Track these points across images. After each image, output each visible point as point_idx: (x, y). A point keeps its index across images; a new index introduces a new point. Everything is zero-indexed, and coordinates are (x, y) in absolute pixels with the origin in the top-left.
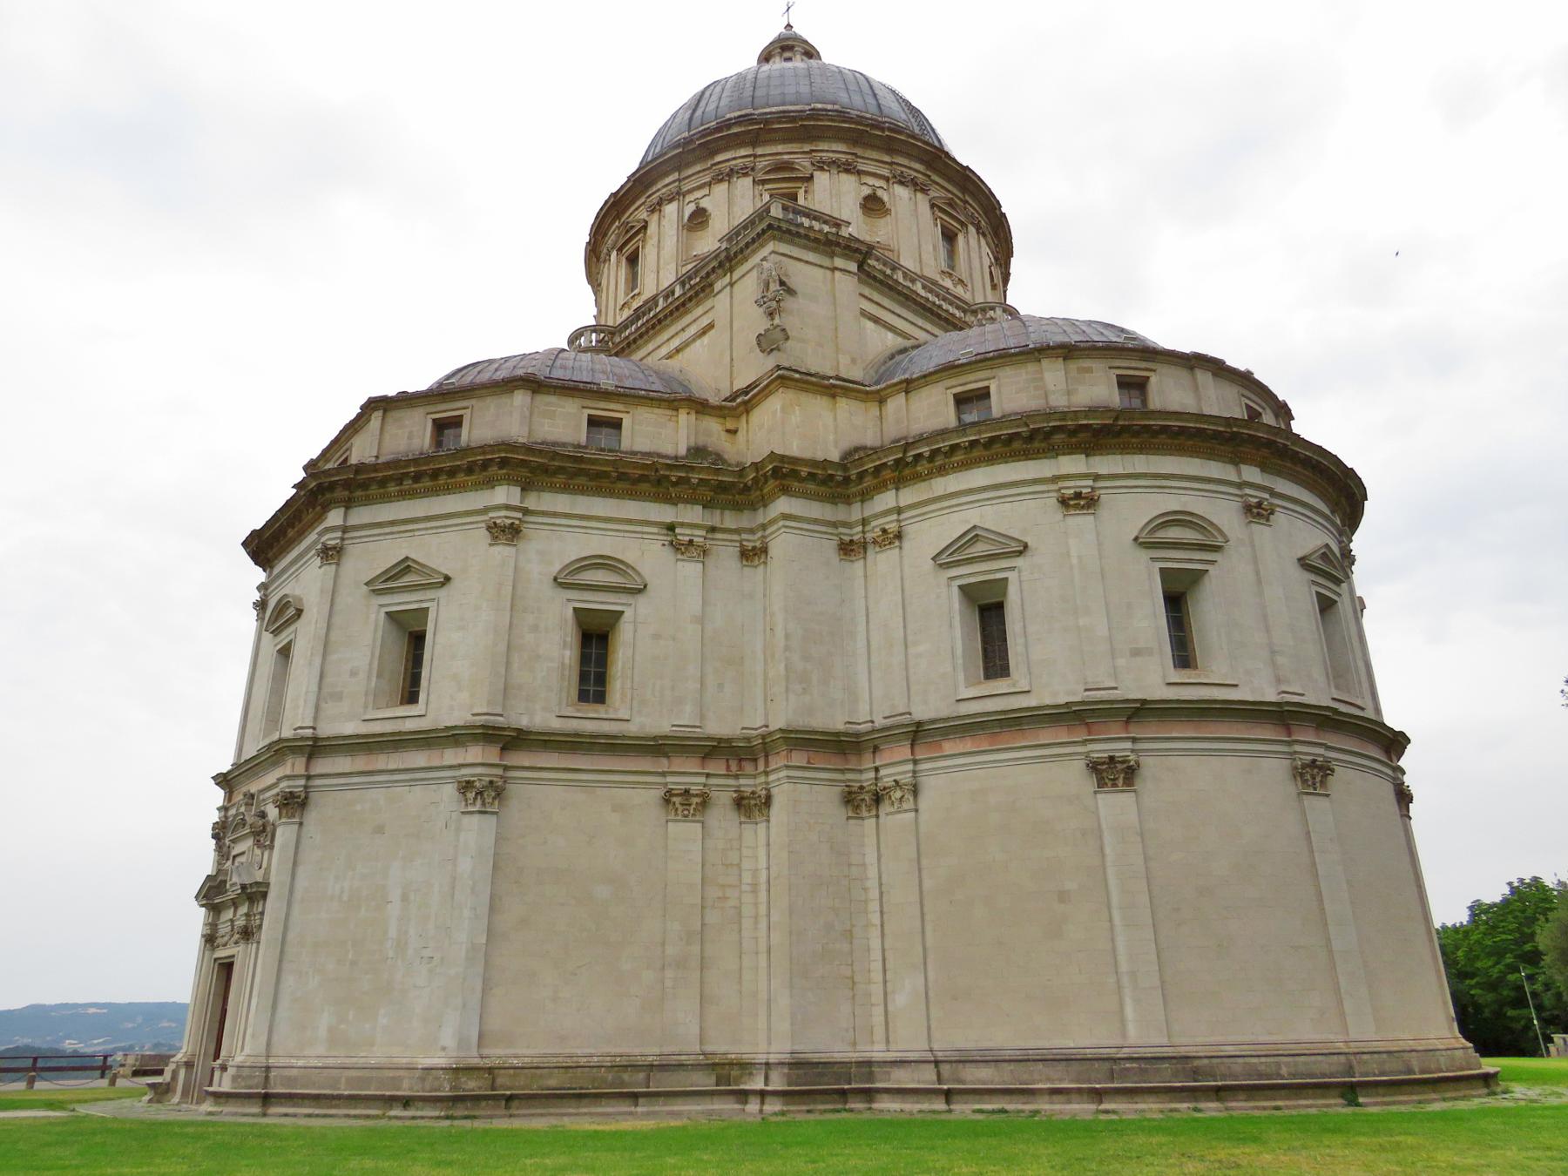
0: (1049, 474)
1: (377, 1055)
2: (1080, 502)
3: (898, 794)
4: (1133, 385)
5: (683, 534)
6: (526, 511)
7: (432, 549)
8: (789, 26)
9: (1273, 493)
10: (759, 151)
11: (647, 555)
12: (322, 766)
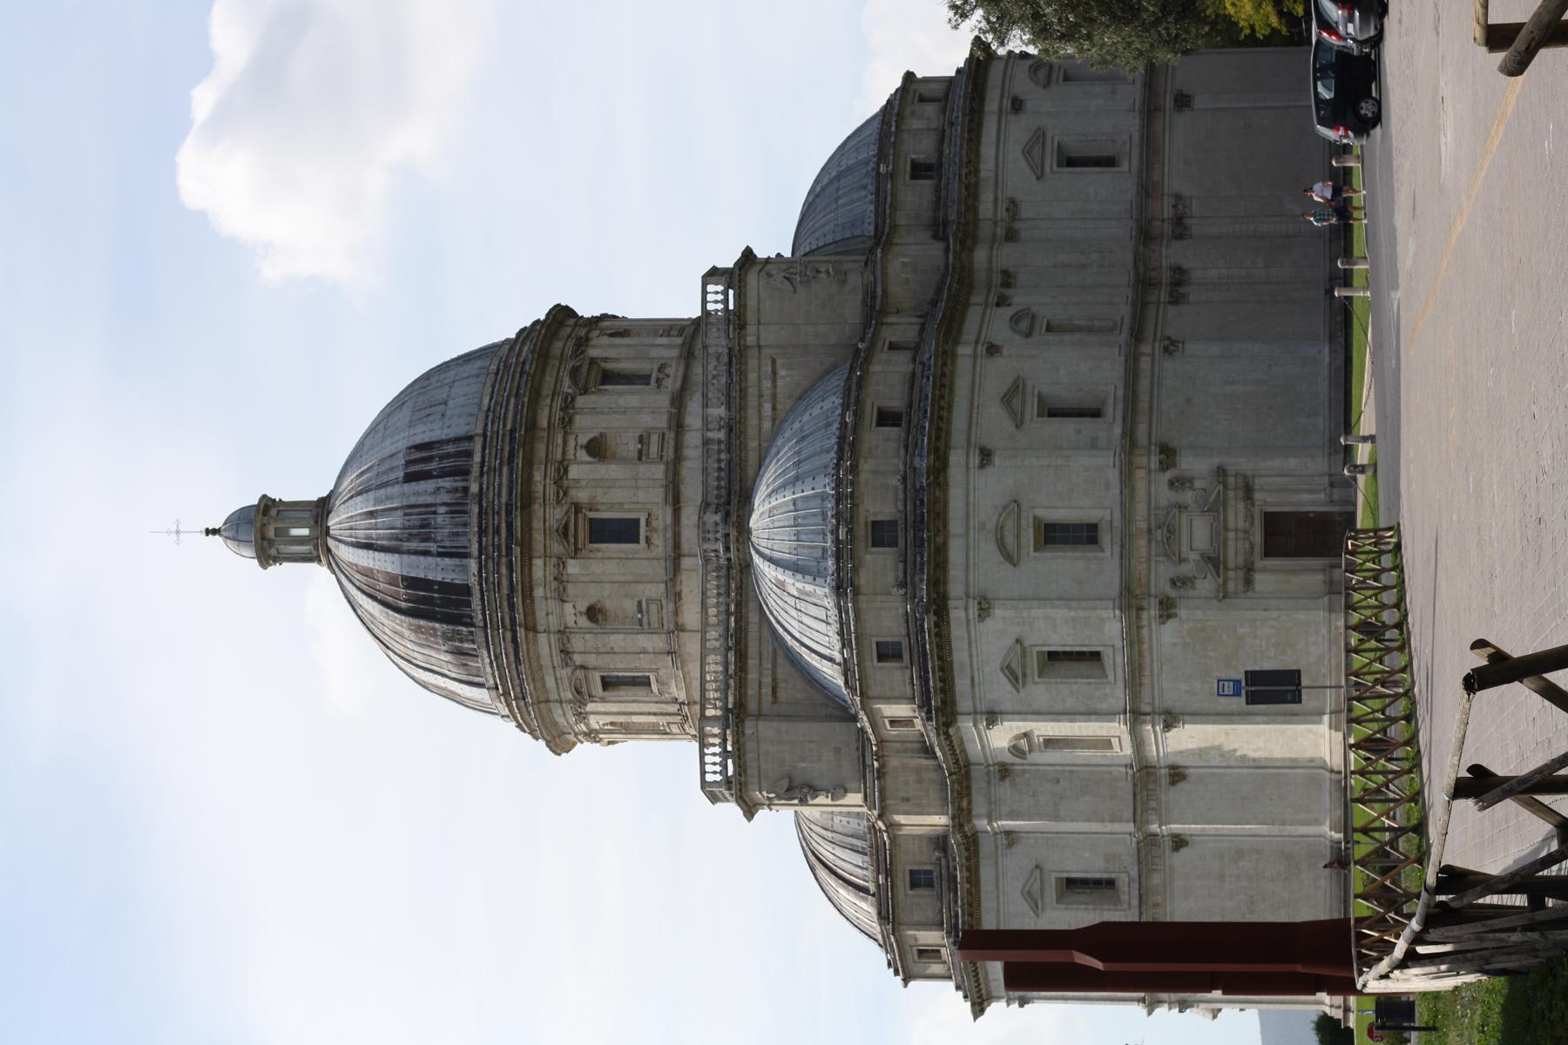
0: (995, 117)
1: (1323, 387)
2: (1017, 105)
4: (922, 99)
5: (993, 299)
6: (977, 342)
8: (208, 532)
10: (547, 390)
11: (1006, 312)
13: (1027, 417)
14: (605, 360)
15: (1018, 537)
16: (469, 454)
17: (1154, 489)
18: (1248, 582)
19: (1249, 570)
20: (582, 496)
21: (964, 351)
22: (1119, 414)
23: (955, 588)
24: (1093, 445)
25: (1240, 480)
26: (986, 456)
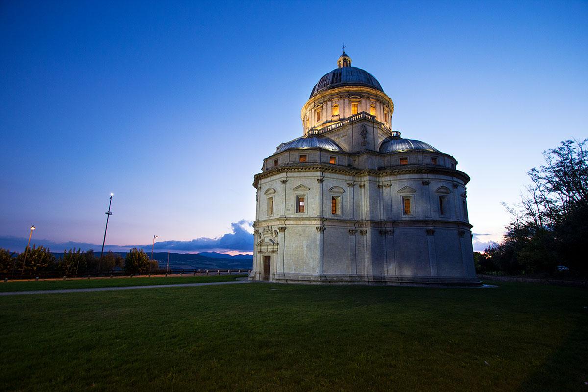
0: (421, 177)
1: (305, 273)
3: (390, 233)
7: (306, 183)
8: (344, 53)
9: (458, 183)
11: (345, 186)
12: (287, 222)
13: (296, 192)
14: (361, 104)
15: (270, 194)
16: (336, 82)
17: (276, 225)
18: (259, 252)
19: (260, 252)
20: (324, 107)
21: (319, 174)
22: (298, 216)
23: (263, 181)
24: (286, 210)
25: (276, 250)
26: (284, 182)
